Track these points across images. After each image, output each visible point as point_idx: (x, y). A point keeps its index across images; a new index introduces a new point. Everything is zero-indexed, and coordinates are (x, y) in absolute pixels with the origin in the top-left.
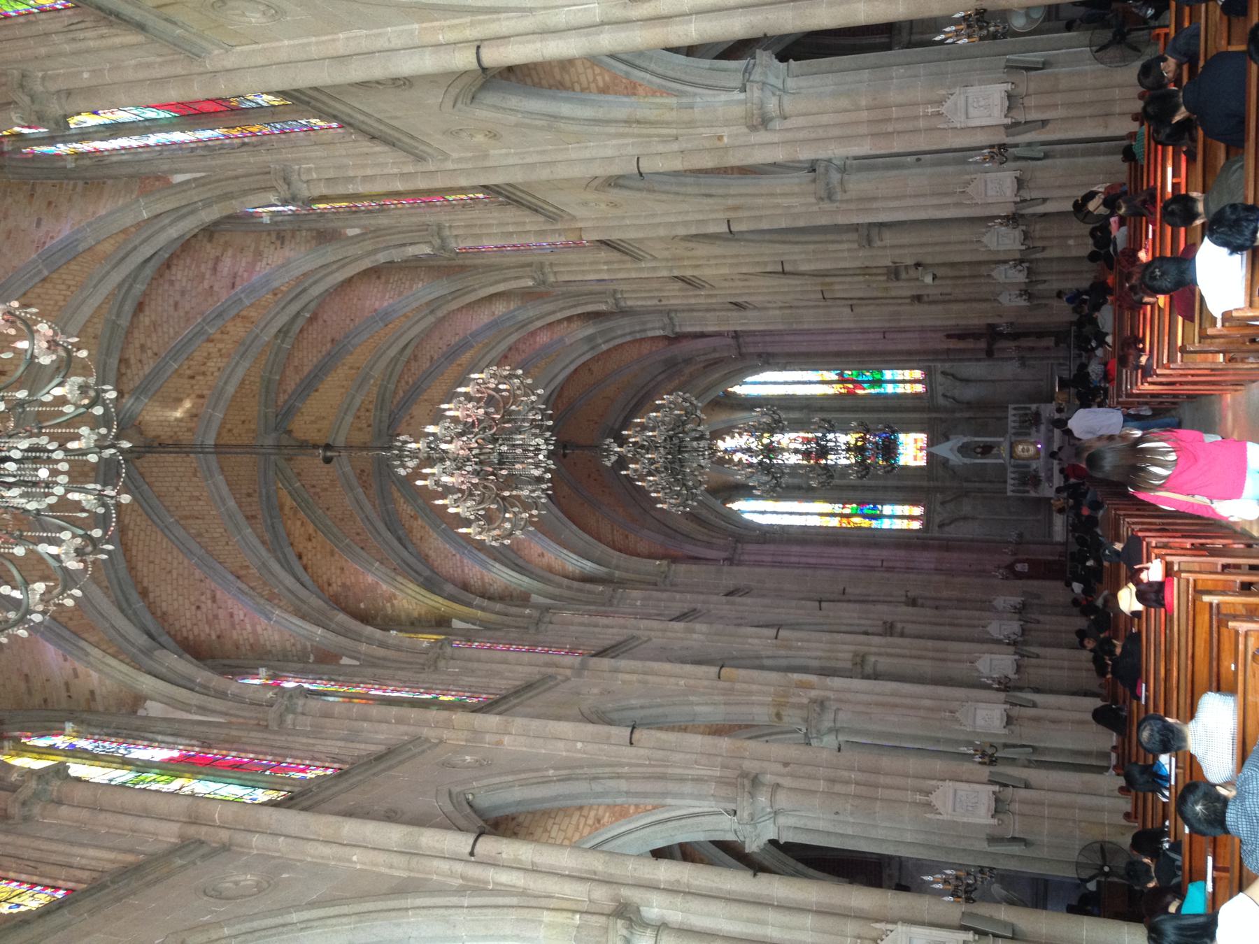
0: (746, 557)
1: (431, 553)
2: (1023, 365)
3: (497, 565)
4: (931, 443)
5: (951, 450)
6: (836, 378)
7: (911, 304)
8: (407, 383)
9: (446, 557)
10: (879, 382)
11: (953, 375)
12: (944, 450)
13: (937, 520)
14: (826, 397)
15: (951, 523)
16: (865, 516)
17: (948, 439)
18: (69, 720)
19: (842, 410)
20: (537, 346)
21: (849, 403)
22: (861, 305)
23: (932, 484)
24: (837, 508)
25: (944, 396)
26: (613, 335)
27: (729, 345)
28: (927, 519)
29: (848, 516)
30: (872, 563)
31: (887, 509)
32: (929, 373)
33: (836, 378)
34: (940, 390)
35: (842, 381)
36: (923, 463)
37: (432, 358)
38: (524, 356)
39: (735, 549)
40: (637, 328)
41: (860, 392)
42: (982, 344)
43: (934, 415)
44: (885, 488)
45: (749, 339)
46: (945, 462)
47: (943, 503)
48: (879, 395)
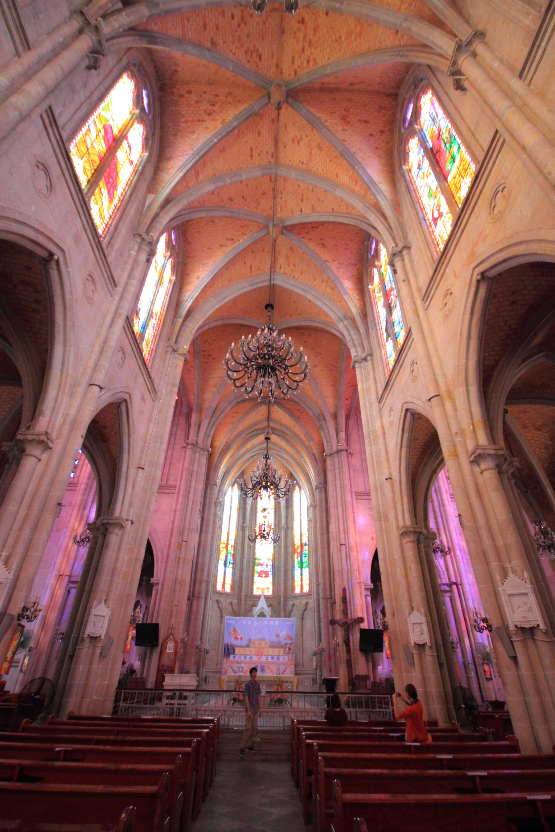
0: (197, 455)
1: (195, 135)
2: (315, 654)
3: (181, 174)
4: (266, 597)
5: (262, 608)
6: (304, 542)
7: (398, 527)
8: (326, 121)
9: (192, 145)
10: (301, 567)
11: (305, 610)
12: (262, 604)
13: (221, 599)
14: (293, 538)
15: (219, 607)
16: (226, 557)
17: (269, 606)
18: (149, 155)
19: (286, 547)
20: (341, 280)
21: (290, 550)
22: (392, 485)
23: (243, 597)
24: (232, 542)
25: (294, 604)
26: (350, 330)
27: (332, 449)
28: (222, 594)
29: (227, 547)
30: (186, 533)
31: (229, 571)
32: (308, 595)
33: (304, 542)
34: (297, 602)
35: (302, 546)
36: (256, 592)
37: (345, 141)
38: (335, 271)
39: (203, 449)
40: (356, 343)
41: (296, 555)
42: (338, 616)
43: (282, 599)
44: (242, 570)
45: (336, 461)
46: (255, 605)
47: (231, 603)
48: (293, 566)
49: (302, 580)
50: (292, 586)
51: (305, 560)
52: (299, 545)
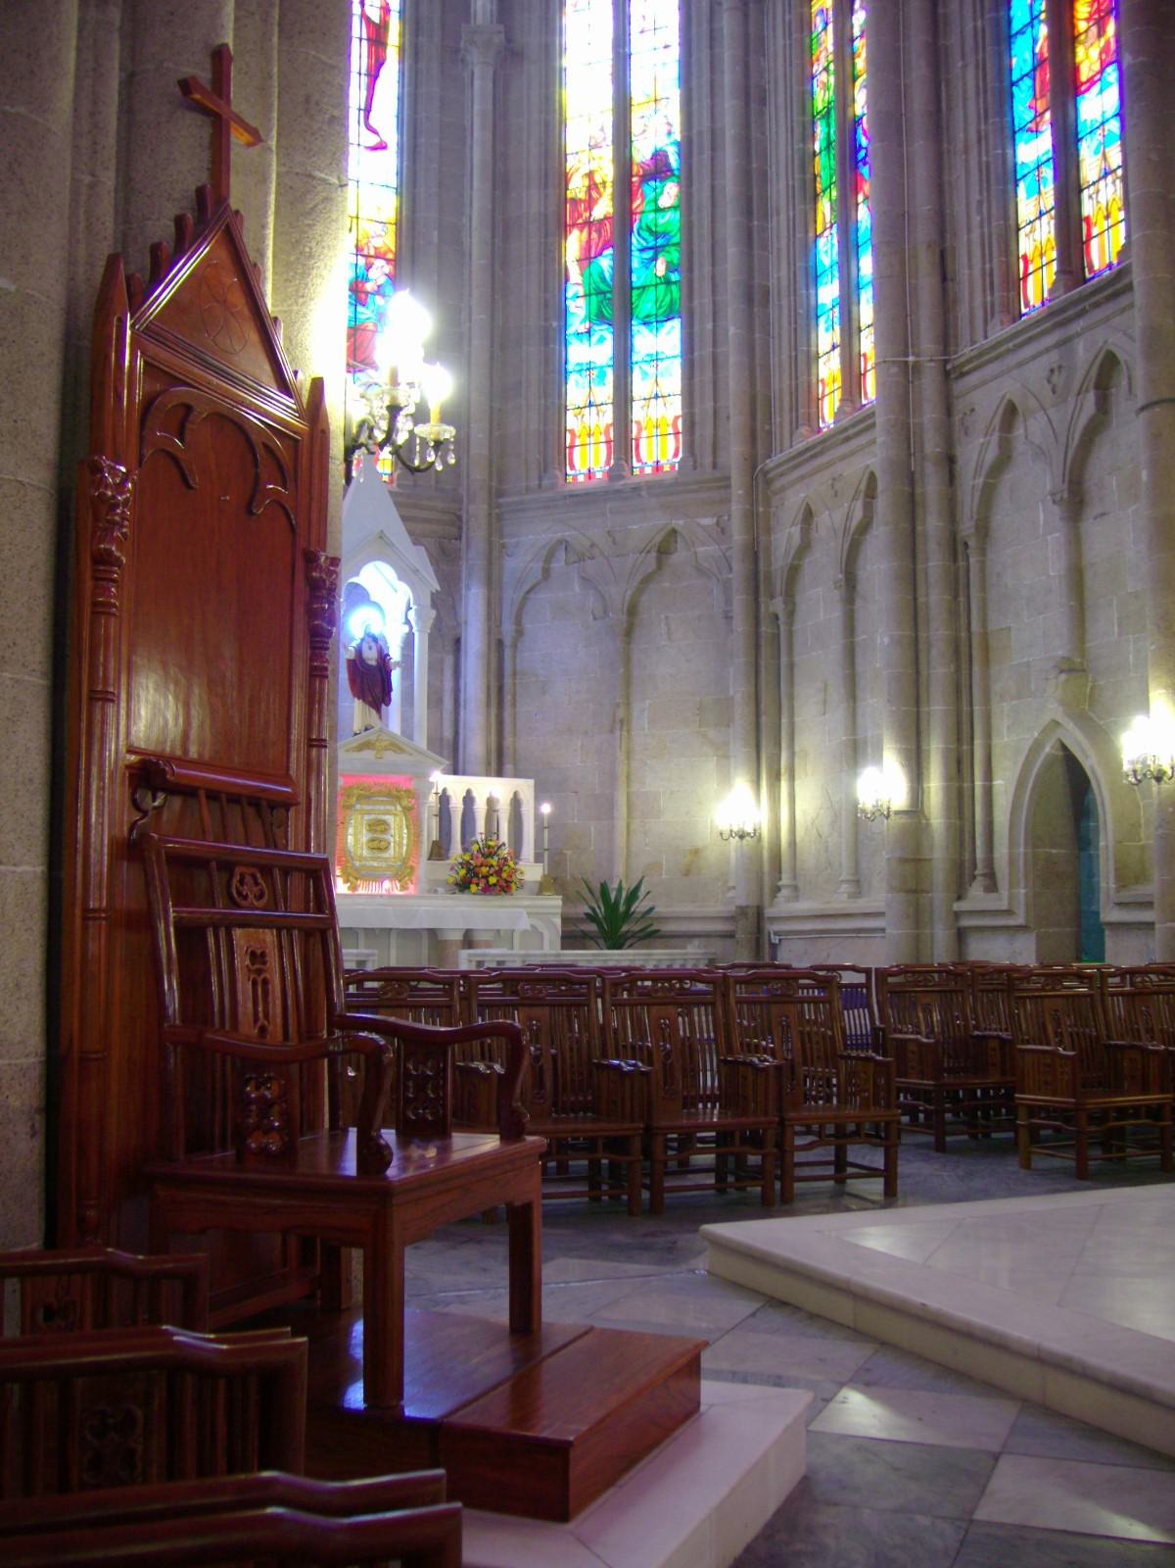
6: (642, 153)
21: (531, 202)
33: (642, 153)
41: (574, 244)
48: (563, 314)
49: (623, 399)
50: (544, 437)
51: (651, 272)
52: (606, 172)
